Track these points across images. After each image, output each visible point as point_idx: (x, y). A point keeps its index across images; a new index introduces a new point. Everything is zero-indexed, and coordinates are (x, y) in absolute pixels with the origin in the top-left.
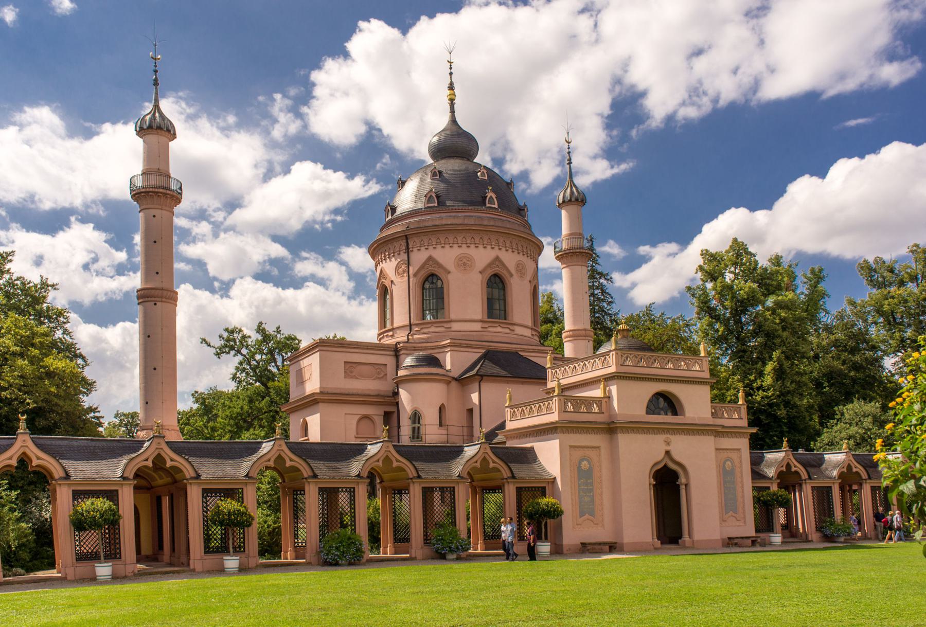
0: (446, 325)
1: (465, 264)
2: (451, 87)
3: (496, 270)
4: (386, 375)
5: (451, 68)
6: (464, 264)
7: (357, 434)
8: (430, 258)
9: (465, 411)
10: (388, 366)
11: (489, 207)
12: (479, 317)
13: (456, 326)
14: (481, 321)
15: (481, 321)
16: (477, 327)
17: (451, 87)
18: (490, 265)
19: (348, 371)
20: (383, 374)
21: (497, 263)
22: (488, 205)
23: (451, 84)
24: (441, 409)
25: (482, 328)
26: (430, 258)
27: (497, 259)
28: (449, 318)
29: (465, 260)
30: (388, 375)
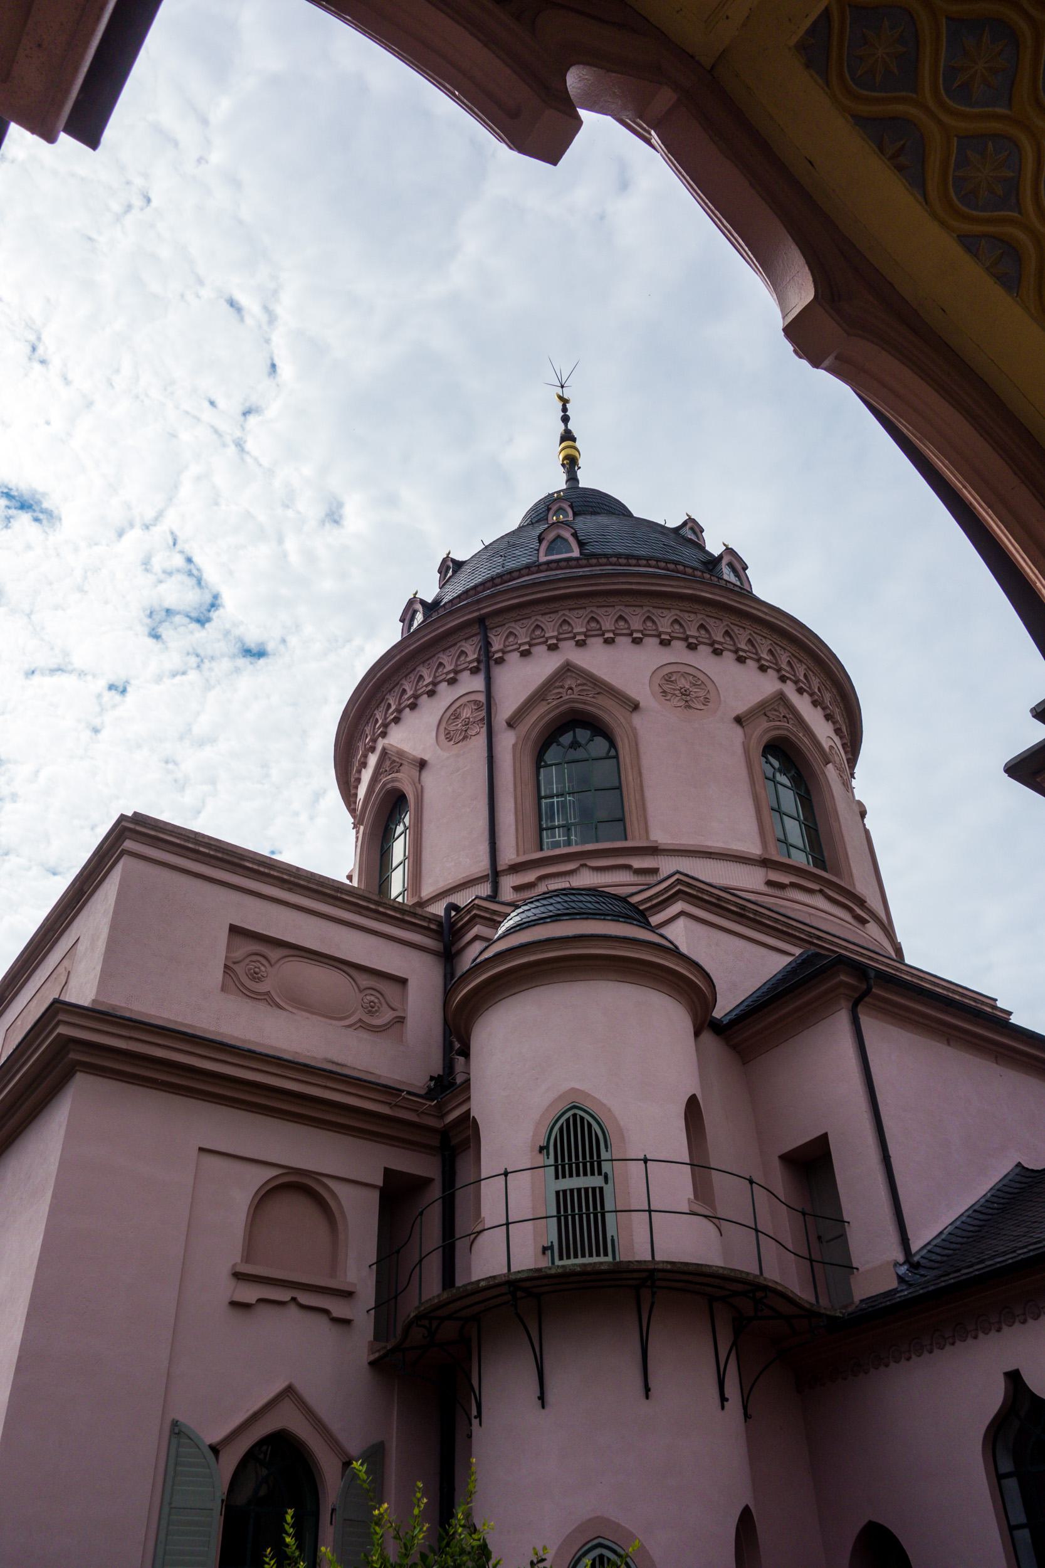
0: (637, 863)
1: (685, 693)
2: (568, 436)
4: (401, 1020)
7: (247, 1257)
8: (568, 669)
9: (776, 1163)
10: (410, 983)
17: (568, 436)
19: (238, 969)
20: (387, 1016)
24: (693, 1108)
26: (568, 669)
28: (648, 838)
29: (683, 683)
30: (410, 1023)
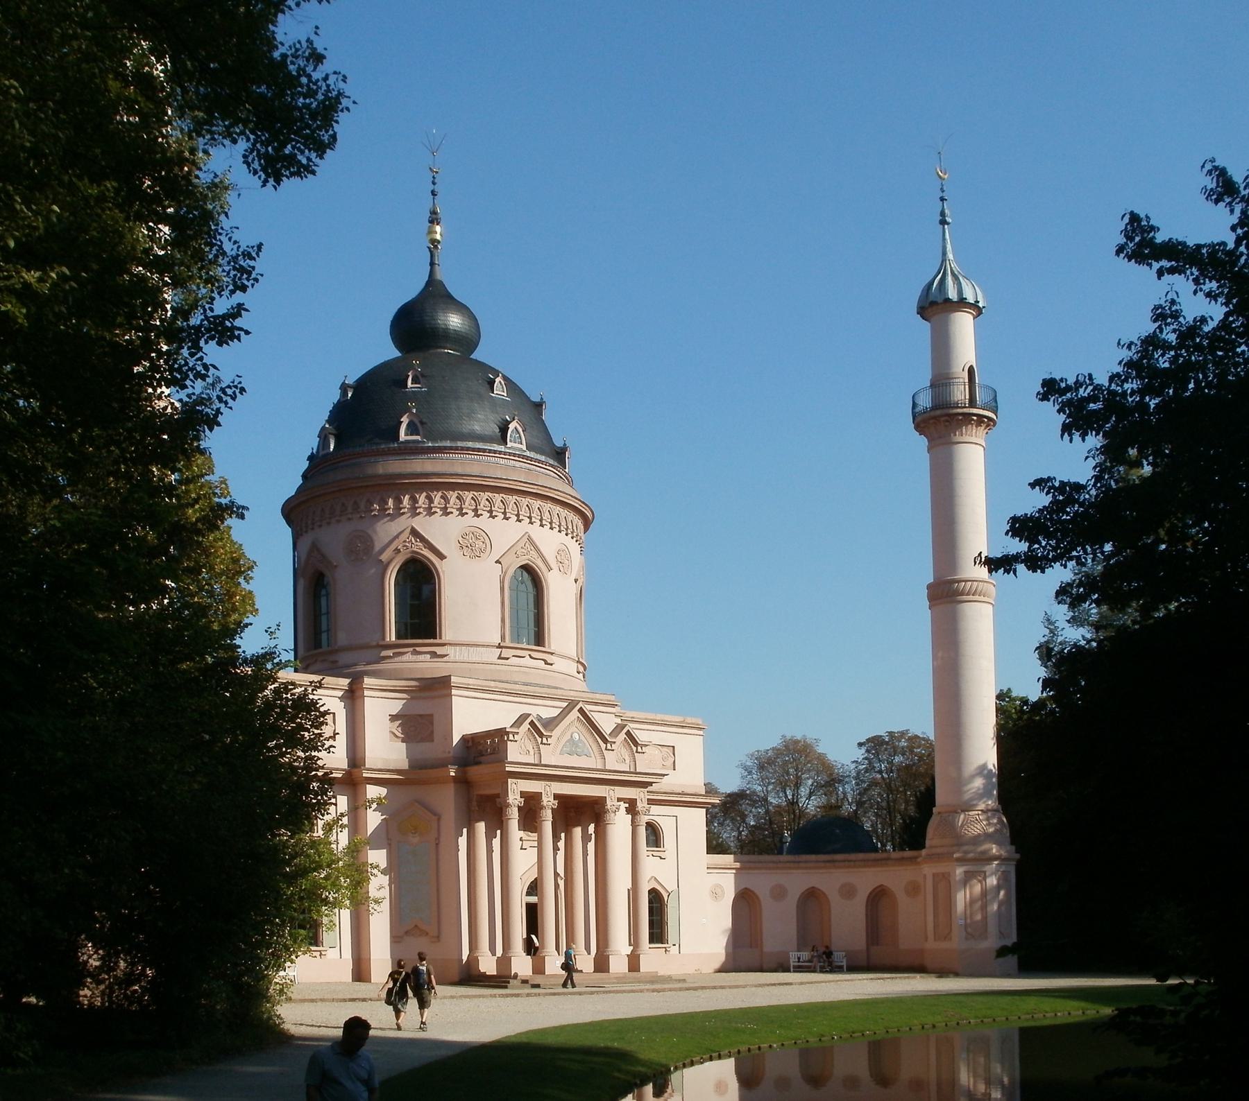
5: (434, 183)
23: (434, 212)
26: (315, 547)
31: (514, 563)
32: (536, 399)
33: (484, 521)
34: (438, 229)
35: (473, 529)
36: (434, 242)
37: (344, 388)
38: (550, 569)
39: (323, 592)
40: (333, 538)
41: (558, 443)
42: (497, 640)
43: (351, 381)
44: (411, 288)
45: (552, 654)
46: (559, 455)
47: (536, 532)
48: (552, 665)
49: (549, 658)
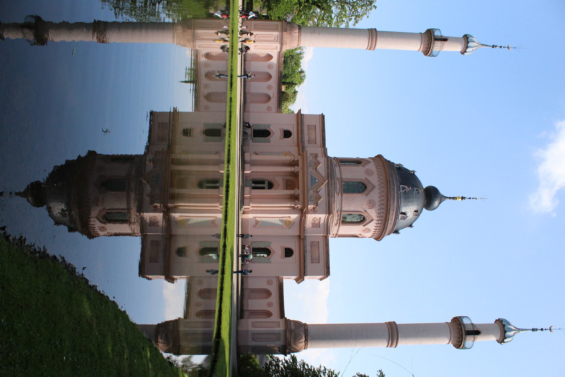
0: (337, 165)
2: (463, 198)
3: (369, 188)
6: (368, 172)
11: (400, 186)
12: (344, 177)
13: (337, 169)
14: (341, 178)
15: (341, 178)
16: (338, 175)
17: (463, 198)
18: (369, 182)
21: (372, 187)
22: (401, 186)
25: (338, 178)
27: (374, 187)
31: (365, 215)
32: (413, 225)
33: (377, 207)
34: (461, 199)
35: (375, 204)
36: (456, 198)
37: (414, 171)
38: (364, 226)
39: (356, 164)
40: (372, 166)
41: (400, 231)
42: (344, 209)
43: (416, 174)
44: (442, 192)
45: (339, 226)
46: (396, 232)
47: (374, 223)
48: (336, 226)
49: (337, 225)
